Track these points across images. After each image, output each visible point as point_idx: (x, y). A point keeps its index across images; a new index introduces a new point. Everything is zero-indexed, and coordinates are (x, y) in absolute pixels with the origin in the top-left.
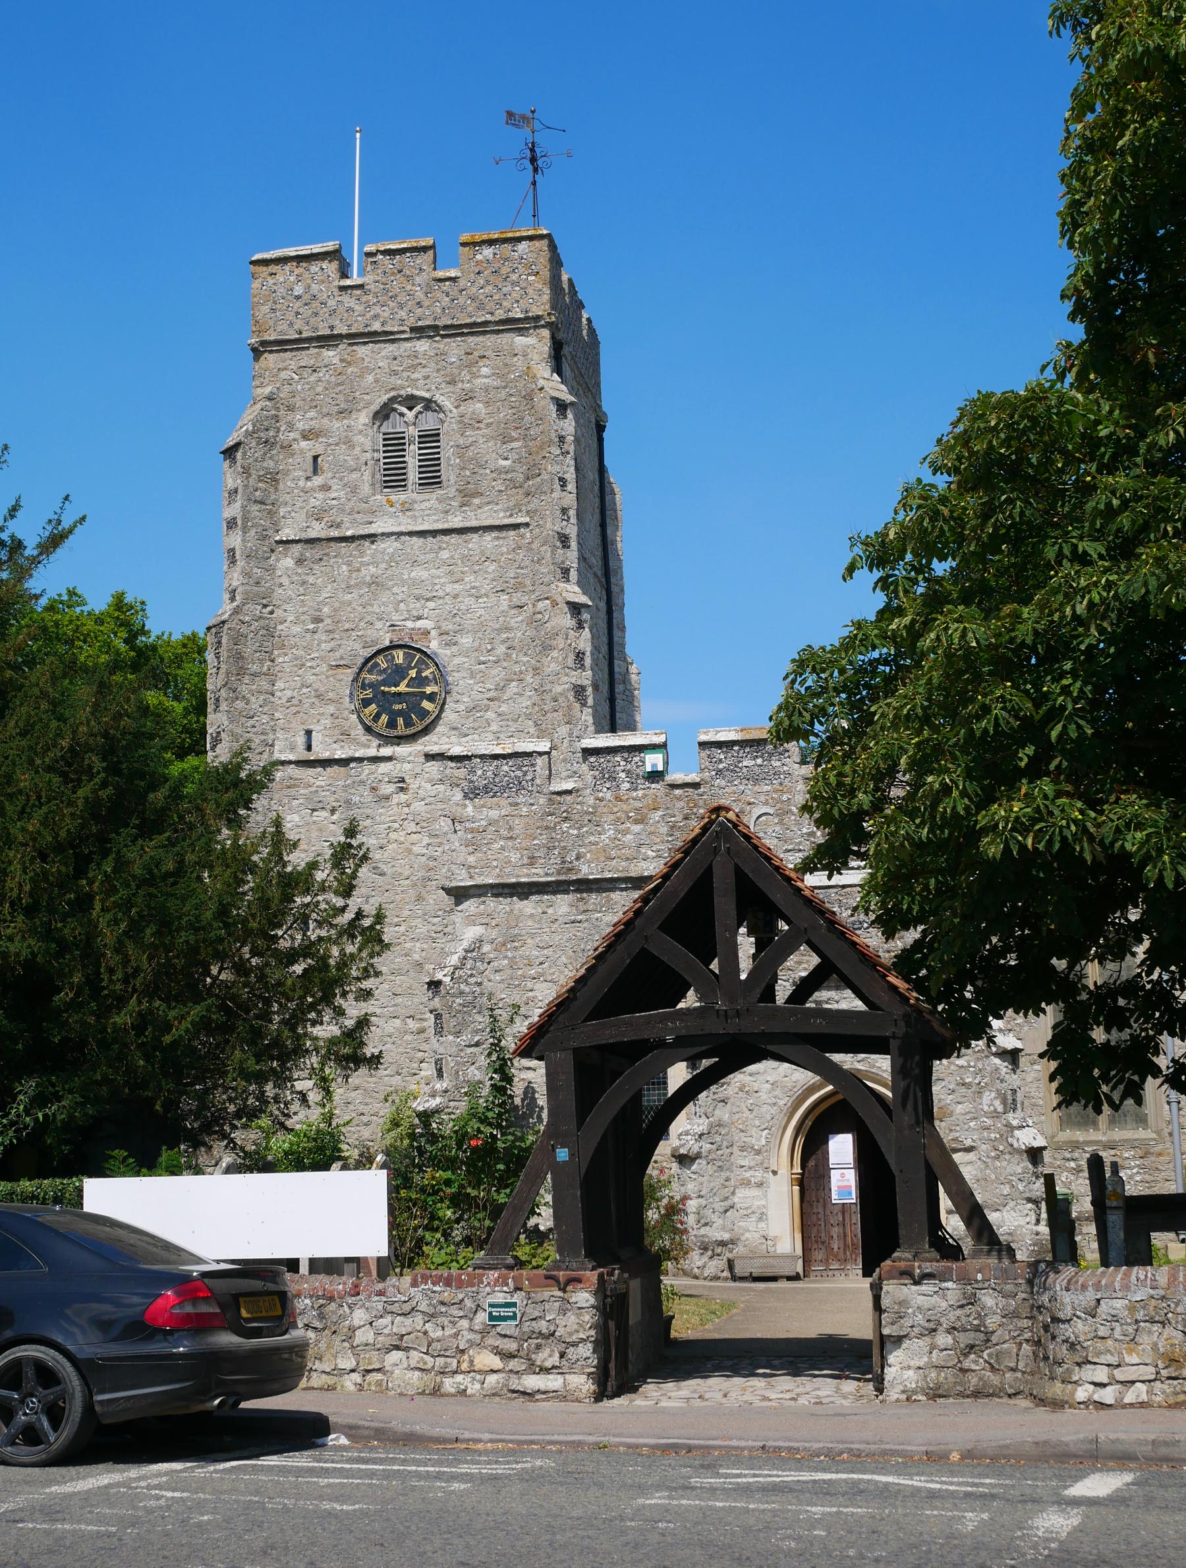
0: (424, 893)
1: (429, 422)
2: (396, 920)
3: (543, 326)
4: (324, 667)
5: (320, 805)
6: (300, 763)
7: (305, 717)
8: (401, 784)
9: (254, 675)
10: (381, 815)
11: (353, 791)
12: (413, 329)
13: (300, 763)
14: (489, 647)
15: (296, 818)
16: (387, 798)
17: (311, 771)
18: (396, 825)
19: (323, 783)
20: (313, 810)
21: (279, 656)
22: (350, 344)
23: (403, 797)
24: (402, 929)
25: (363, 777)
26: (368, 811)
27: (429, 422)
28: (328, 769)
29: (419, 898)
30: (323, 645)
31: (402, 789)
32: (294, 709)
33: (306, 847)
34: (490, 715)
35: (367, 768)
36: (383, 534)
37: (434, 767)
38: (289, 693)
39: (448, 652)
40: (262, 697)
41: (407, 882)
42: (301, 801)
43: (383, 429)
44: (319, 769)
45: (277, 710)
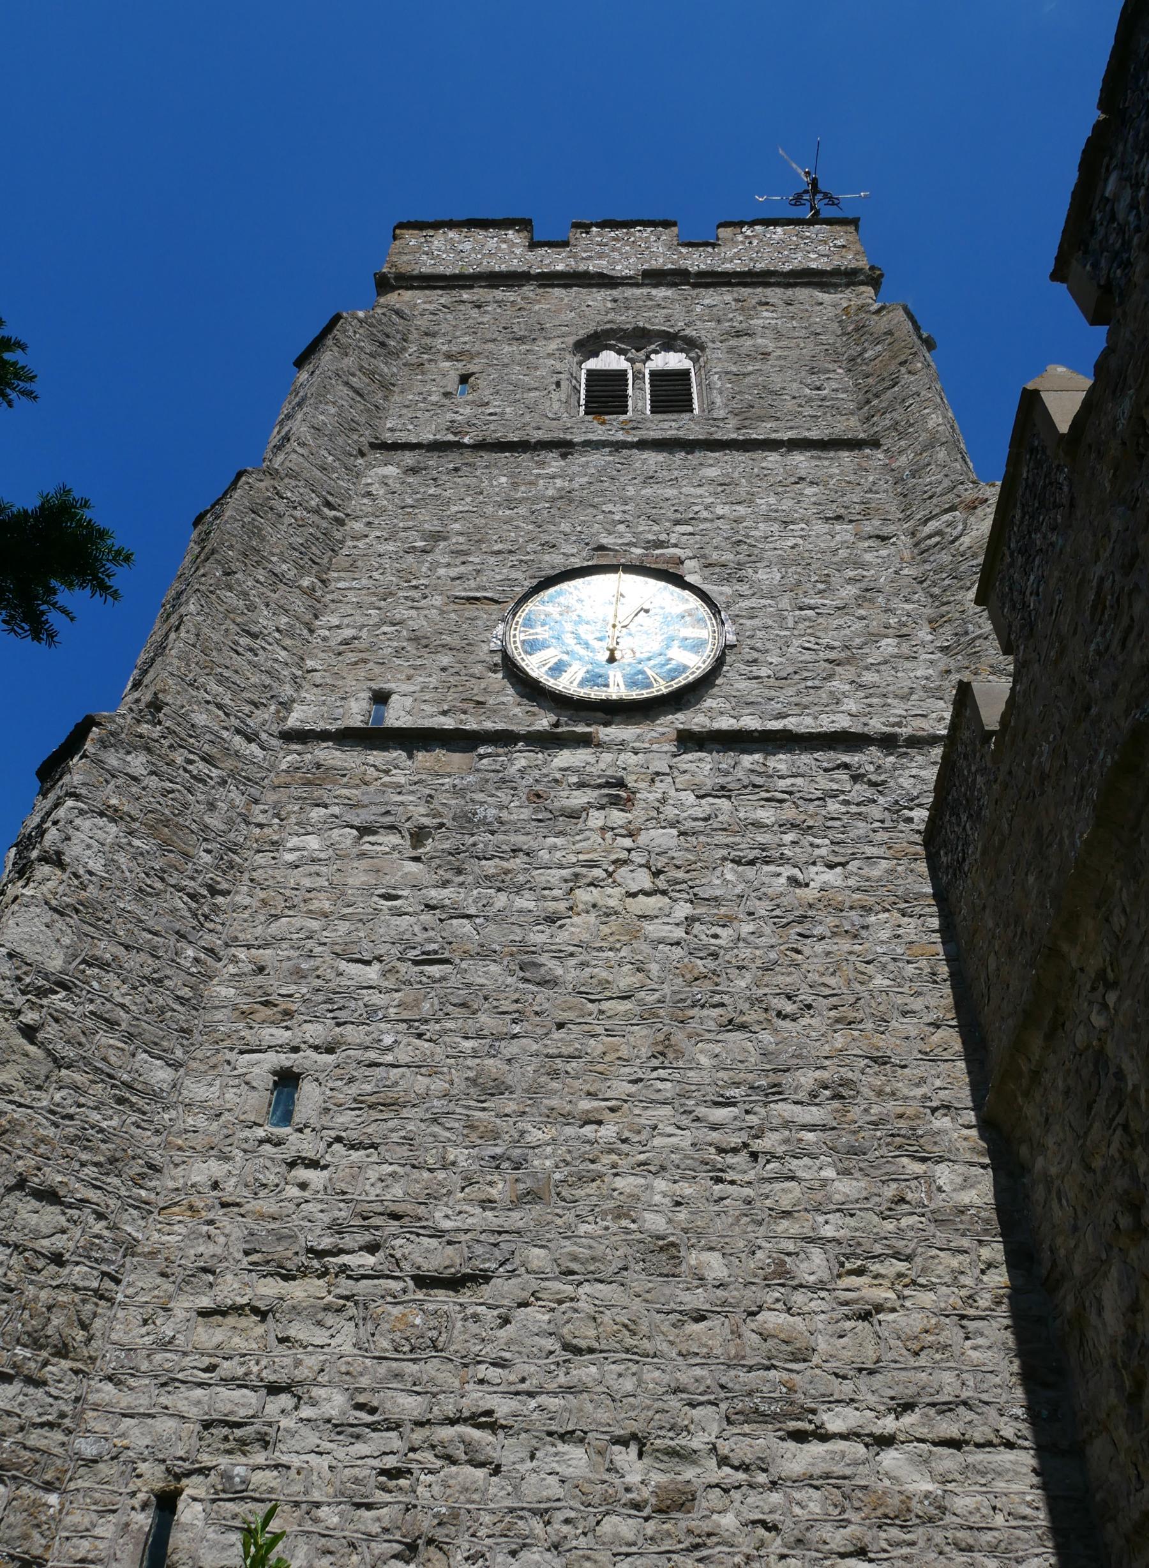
0: (679, 1037)
1: (674, 361)
2: (586, 1104)
3: (862, 283)
4: (438, 600)
5: (388, 820)
6: (348, 737)
7: (377, 670)
8: (617, 792)
9: (278, 577)
10: (553, 849)
11: (480, 796)
12: (647, 274)
13: (348, 737)
14: (821, 586)
15: (313, 843)
16: (574, 815)
17: (377, 757)
18: (598, 873)
19: (402, 780)
20: (365, 830)
21: (339, 579)
22: (540, 286)
23: (617, 817)
24: (608, 1132)
25: (512, 770)
26: (519, 840)
27: (674, 361)
28: (420, 755)
29: (663, 1051)
30: (442, 571)
31: (615, 801)
32: (352, 657)
33: (327, 906)
34: (836, 685)
35: (522, 759)
36: (587, 444)
37: (702, 766)
38: (348, 633)
39: (727, 590)
40: (284, 620)
41: (627, 1005)
42: (336, 810)
43: (592, 364)
44: (399, 755)
45: (314, 656)
